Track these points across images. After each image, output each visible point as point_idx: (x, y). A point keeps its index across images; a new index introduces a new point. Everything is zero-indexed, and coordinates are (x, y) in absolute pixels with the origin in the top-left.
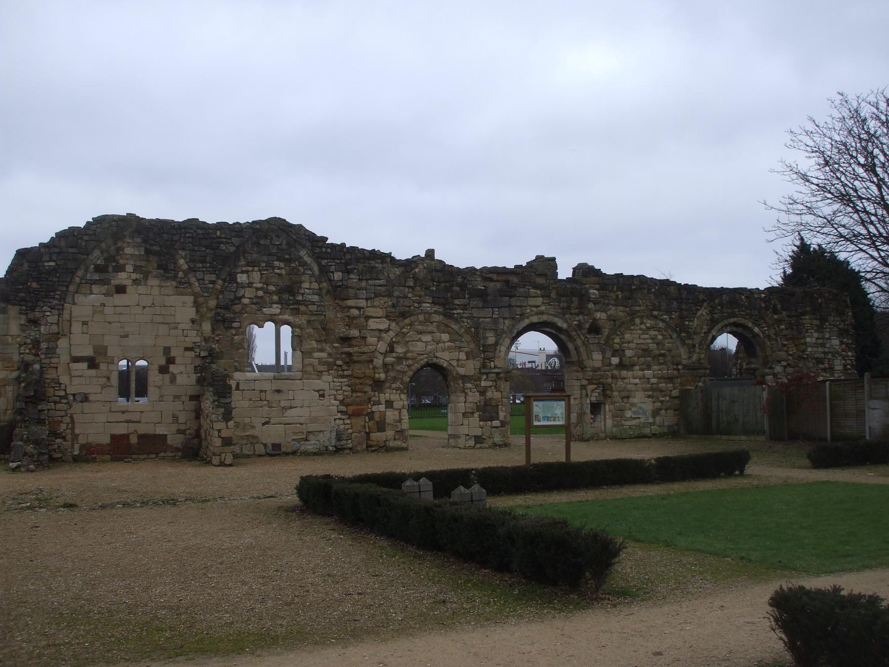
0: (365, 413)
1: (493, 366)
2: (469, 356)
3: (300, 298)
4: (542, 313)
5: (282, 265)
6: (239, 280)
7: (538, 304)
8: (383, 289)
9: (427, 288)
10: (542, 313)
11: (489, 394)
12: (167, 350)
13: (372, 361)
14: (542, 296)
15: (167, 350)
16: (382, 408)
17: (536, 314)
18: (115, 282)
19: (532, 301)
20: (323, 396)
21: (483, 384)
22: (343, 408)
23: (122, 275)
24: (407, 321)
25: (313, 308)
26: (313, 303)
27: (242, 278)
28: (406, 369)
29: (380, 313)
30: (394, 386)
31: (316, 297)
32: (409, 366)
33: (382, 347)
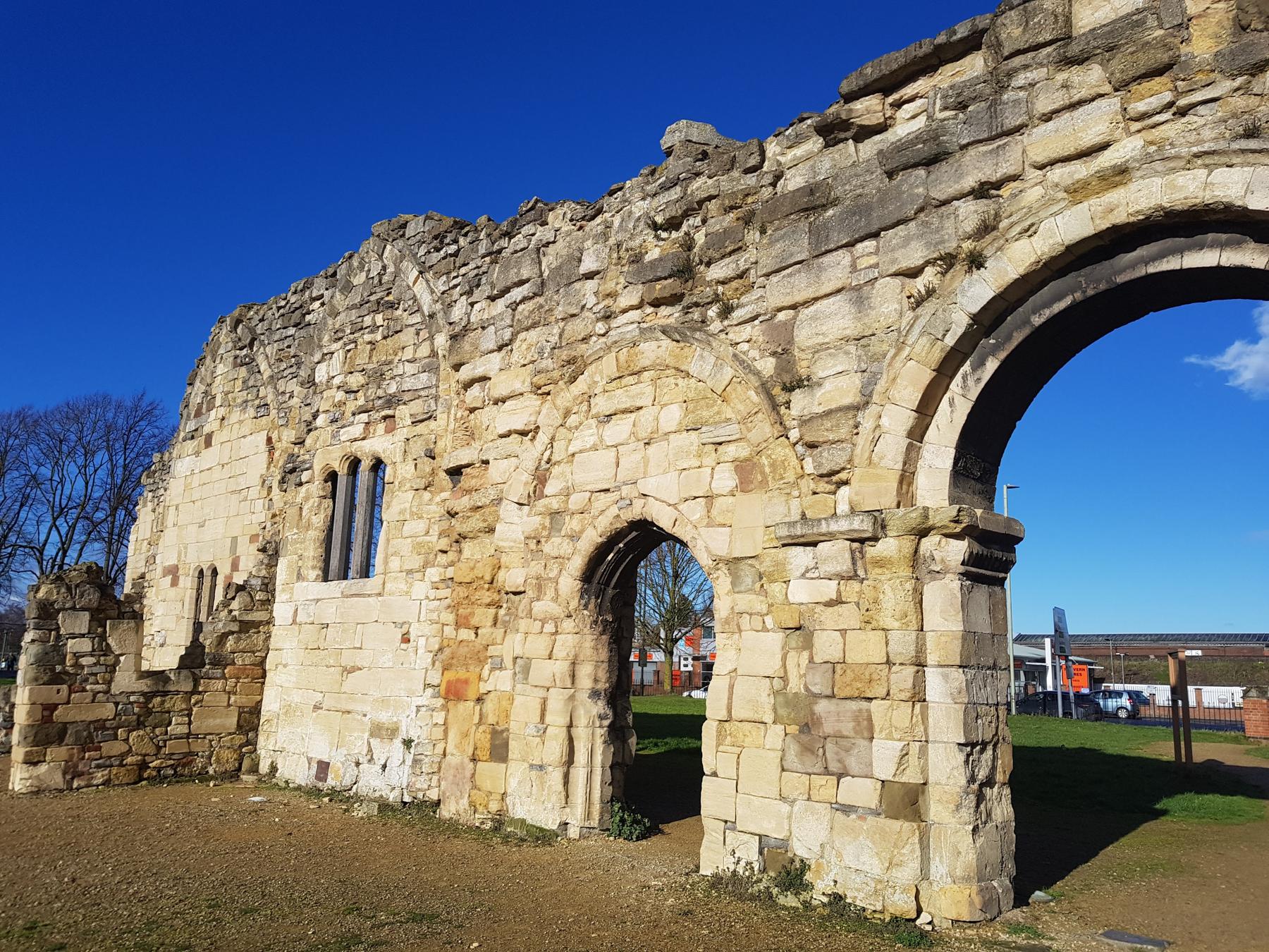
0: (472, 694)
1: (843, 508)
2: (746, 473)
3: (392, 389)
4: (1121, 173)
5: (379, 319)
6: (317, 381)
7: (1089, 138)
8: (530, 305)
9: (637, 259)
10: (1121, 173)
11: (827, 645)
12: (235, 539)
13: (491, 530)
14: (1121, 86)
15: (235, 539)
16: (501, 681)
17: (1077, 192)
18: (206, 430)
19: (1044, 141)
20: (406, 639)
21: (800, 592)
22: (435, 677)
23: (213, 413)
24: (581, 384)
25: (417, 407)
26: (416, 394)
27: (321, 374)
28: (566, 547)
29: (518, 381)
30: (538, 607)
31: (424, 376)
32: (574, 537)
33: (520, 485)
